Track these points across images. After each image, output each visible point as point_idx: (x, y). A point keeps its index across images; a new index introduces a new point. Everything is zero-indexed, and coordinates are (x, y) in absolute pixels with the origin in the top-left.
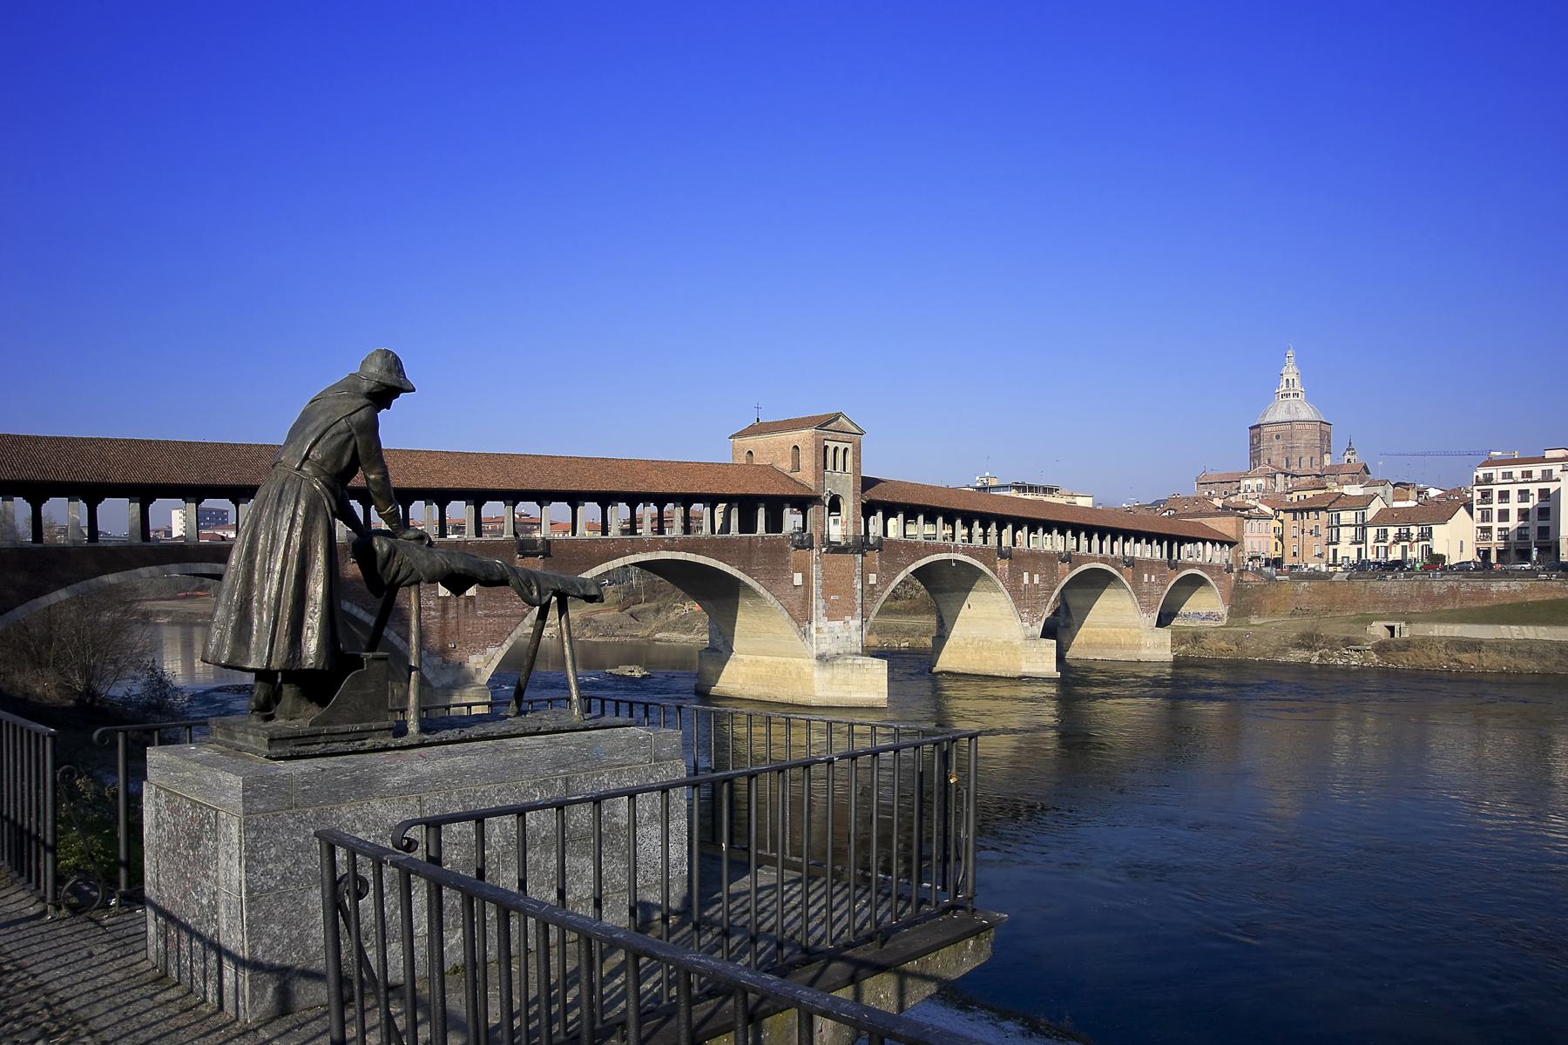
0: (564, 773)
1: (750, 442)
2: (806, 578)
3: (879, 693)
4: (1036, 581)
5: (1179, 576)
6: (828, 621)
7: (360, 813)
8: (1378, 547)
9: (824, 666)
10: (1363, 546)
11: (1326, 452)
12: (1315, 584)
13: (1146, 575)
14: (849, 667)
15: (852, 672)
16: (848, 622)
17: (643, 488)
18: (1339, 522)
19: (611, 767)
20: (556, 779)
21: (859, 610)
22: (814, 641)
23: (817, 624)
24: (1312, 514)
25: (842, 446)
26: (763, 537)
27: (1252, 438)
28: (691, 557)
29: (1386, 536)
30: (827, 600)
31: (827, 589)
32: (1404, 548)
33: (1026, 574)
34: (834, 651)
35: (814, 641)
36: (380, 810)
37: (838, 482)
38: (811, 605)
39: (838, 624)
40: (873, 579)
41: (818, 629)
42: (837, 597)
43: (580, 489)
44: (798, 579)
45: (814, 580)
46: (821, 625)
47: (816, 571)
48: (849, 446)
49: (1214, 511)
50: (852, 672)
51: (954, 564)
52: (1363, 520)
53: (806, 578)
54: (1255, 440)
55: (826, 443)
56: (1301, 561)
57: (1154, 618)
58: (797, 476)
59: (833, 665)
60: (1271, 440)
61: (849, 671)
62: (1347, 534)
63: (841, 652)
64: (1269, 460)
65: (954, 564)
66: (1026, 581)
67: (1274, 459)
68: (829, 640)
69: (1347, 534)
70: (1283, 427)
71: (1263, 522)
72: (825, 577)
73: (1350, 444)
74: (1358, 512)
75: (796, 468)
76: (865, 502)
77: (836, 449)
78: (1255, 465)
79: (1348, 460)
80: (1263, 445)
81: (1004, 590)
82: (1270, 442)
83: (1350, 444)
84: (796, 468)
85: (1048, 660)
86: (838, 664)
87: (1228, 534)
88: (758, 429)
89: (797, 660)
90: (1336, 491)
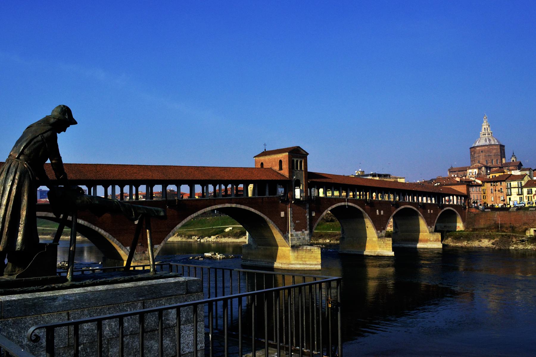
0: (142, 300)
1: (262, 159)
2: (286, 214)
3: (317, 261)
5: (443, 210)
6: (296, 231)
7: (36, 320)
8: (528, 197)
9: (294, 251)
12: (502, 213)
13: (429, 210)
14: (305, 250)
15: (306, 253)
16: (304, 232)
17: (218, 178)
18: (510, 186)
19: (166, 297)
20: (138, 302)
21: (308, 227)
22: (290, 240)
23: (291, 232)
24: (499, 184)
26: (268, 197)
27: (471, 152)
28: (239, 206)
29: (532, 192)
30: (295, 223)
31: (294, 219)
34: (298, 244)
35: (290, 240)
36: (47, 319)
37: (298, 174)
39: (300, 232)
41: (292, 235)
42: (299, 221)
43: (193, 179)
44: (282, 214)
45: (289, 215)
46: (293, 233)
49: (456, 183)
50: (306, 253)
51: (347, 207)
52: (521, 185)
54: (473, 153)
56: (495, 203)
57: (433, 228)
58: (281, 172)
59: (298, 250)
60: (479, 153)
61: (305, 252)
62: (515, 191)
63: (301, 244)
66: (378, 213)
67: (481, 161)
68: (296, 240)
69: (515, 191)
71: (478, 188)
73: (513, 154)
74: (519, 182)
75: (281, 168)
77: (297, 161)
78: (473, 163)
80: (476, 155)
81: (369, 217)
82: (479, 154)
83: (513, 154)
84: (281, 168)
85: (389, 246)
86: (300, 250)
88: (265, 153)
89: (283, 248)
90: (509, 173)
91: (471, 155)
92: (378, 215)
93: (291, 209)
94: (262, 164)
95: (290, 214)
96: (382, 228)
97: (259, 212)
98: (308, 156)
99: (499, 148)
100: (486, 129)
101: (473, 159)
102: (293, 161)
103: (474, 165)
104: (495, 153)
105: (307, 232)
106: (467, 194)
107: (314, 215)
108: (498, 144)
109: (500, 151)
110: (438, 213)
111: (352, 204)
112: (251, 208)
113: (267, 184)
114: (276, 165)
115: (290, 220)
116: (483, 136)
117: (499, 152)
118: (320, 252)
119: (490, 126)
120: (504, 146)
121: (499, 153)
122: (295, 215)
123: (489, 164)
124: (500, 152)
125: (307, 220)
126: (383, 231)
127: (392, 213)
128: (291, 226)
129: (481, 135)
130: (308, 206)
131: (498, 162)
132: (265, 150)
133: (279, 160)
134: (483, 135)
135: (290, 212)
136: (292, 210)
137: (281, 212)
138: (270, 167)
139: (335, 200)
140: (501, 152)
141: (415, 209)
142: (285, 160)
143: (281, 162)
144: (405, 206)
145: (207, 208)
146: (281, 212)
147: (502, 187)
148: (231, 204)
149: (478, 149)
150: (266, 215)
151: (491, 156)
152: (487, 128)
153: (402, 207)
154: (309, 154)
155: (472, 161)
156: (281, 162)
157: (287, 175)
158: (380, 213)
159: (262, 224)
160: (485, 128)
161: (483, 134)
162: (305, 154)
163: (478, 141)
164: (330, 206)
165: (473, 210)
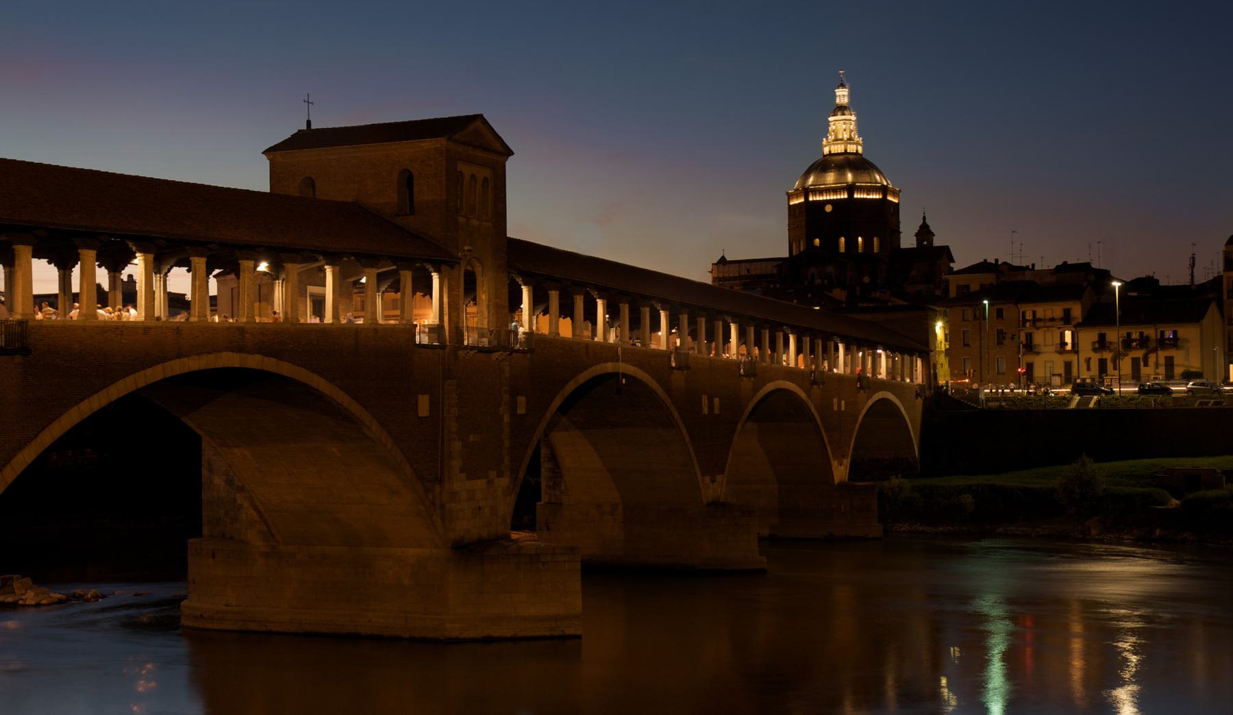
5: (870, 403)
6: (468, 478)
10: (1074, 358)
13: (835, 400)
21: (507, 460)
32: (1135, 362)
39: (480, 484)
40: (521, 410)
44: (424, 405)
53: (433, 404)
55: (461, 167)
66: (706, 410)
73: (924, 218)
77: (473, 176)
83: (924, 218)
92: (704, 415)
97: (342, 393)
98: (510, 164)
105: (504, 482)
107: (521, 410)
111: (636, 369)
112: (316, 377)
118: (579, 567)
126: (719, 478)
130: (507, 375)
132: (309, 123)
137: (420, 397)
141: (803, 395)
145: (149, 371)
146: (420, 397)
148: (244, 355)
153: (770, 387)
154: (512, 153)
156: (408, 180)
158: (711, 407)
162: (500, 153)
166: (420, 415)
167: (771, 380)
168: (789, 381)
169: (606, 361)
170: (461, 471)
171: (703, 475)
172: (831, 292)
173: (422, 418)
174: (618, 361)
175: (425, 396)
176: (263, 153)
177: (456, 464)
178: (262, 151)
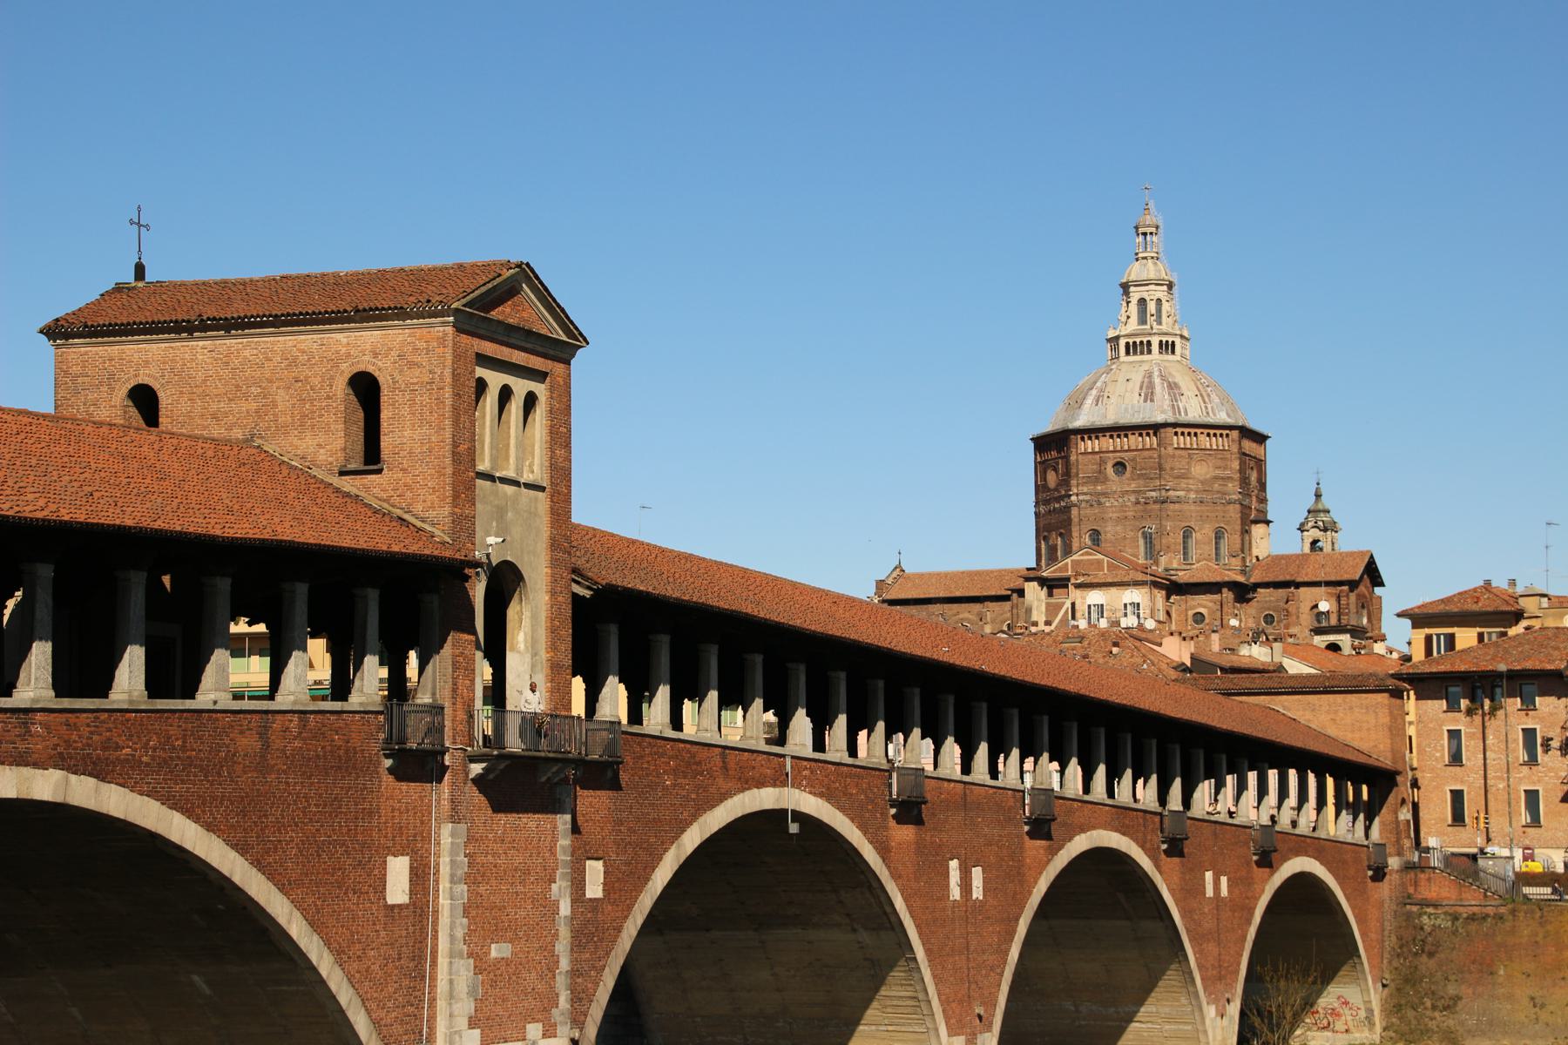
2: (421, 877)
4: (977, 893)
11: (1256, 522)
13: (1209, 875)
25: (521, 387)
27: (1041, 468)
28: (85, 792)
30: (481, 965)
33: (954, 864)
38: (433, 979)
40: (594, 890)
47: (447, 840)
48: (540, 389)
51: (794, 828)
53: (421, 877)
54: (1052, 478)
57: (1232, 1018)
60: (1100, 477)
64: (1096, 536)
65: (794, 828)
66: (955, 893)
67: (1110, 531)
70: (1134, 441)
72: (475, 876)
73: (1318, 496)
76: (587, 593)
77: (505, 394)
78: (1052, 550)
79: (1314, 543)
80: (1079, 493)
82: (1096, 481)
83: (1318, 496)
87: (1364, 747)
91: (1040, 488)
93: (463, 827)
94: (145, 400)
95: (453, 880)
96: (980, 1010)
97: (233, 854)
98: (579, 360)
99: (1235, 449)
100: (1152, 307)
101: (1053, 519)
102: (481, 386)
103: (1069, 560)
104: (1202, 482)
106: (1394, 761)
107: (594, 890)
108: (1230, 421)
109: (1242, 471)
110: (1257, 899)
113: (373, 596)
114: (304, 422)
115: (452, 937)
116: (1132, 358)
117: (1230, 478)
119: (1175, 289)
120: (1261, 438)
121: (1233, 488)
122: (482, 889)
123: (1163, 560)
124: (1237, 476)
125: (556, 936)
127: (1030, 893)
128: (451, 996)
129: (1115, 348)
131: (1224, 550)
132: (140, 271)
133: (348, 370)
134: (1128, 353)
135: (453, 862)
136: (461, 840)
137: (390, 859)
138: (238, 434)
139: (725, 768)
140: (1244, 481)
141: (1145, 862)
142: (414, 376)
143: (366, 389)
144: (1095, 833)
146: (390, 859)
147: (1542, 720)
149: (1090, 445)
150: (282, 889)
151: (1178, 501)
152: (1159, 300)
153: (1080, 844)
155: (1043, 532)
156: (366, 389)
157: (431, 514)
159: (196, 978)
160: (1142, 302)
161: (1127, 344)
163: (1094, 392)
164: (694, 817)
165: (1439, 888)
166: (390, 901)
167: (1083, 829)
168: (1116, 830)
169: (760, 784)
170: (473, 1024)
171: (952, 1032)
172: (1160, 645)
173: (393, 906)
174: (784, 784)
175: (400, 858)
176: (41, 332)
177: (465, 1007)
178: (42, 325)
